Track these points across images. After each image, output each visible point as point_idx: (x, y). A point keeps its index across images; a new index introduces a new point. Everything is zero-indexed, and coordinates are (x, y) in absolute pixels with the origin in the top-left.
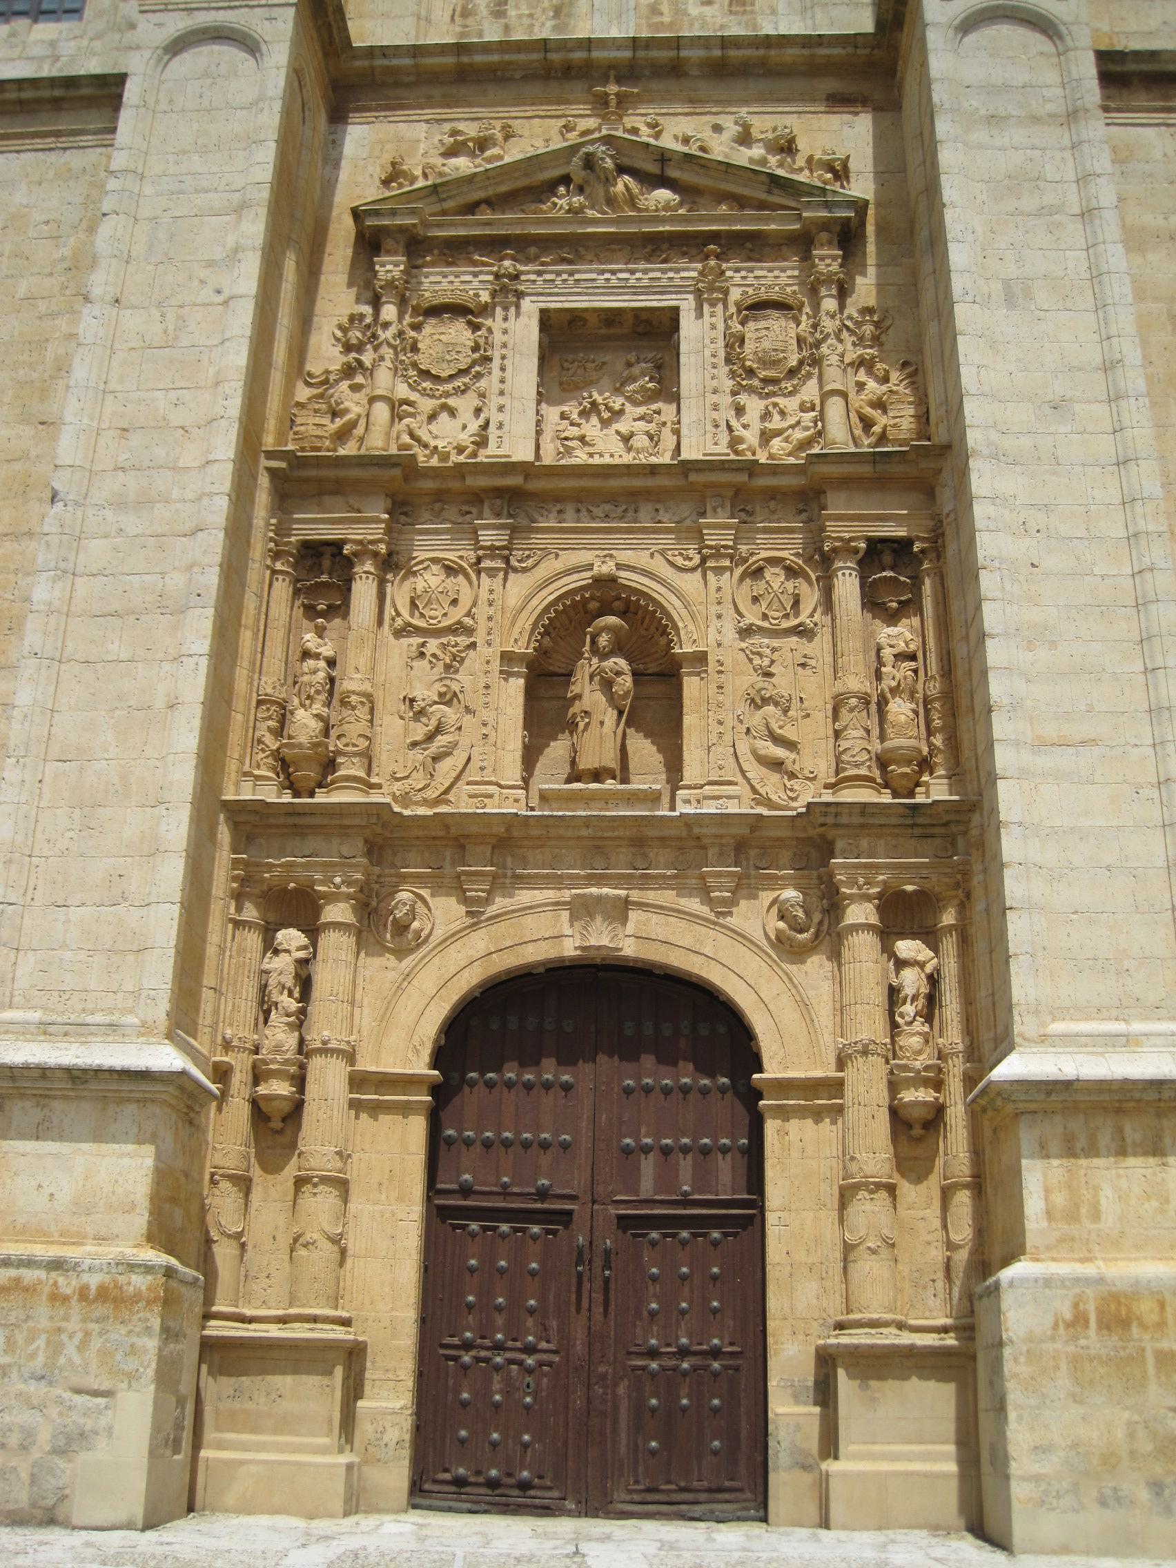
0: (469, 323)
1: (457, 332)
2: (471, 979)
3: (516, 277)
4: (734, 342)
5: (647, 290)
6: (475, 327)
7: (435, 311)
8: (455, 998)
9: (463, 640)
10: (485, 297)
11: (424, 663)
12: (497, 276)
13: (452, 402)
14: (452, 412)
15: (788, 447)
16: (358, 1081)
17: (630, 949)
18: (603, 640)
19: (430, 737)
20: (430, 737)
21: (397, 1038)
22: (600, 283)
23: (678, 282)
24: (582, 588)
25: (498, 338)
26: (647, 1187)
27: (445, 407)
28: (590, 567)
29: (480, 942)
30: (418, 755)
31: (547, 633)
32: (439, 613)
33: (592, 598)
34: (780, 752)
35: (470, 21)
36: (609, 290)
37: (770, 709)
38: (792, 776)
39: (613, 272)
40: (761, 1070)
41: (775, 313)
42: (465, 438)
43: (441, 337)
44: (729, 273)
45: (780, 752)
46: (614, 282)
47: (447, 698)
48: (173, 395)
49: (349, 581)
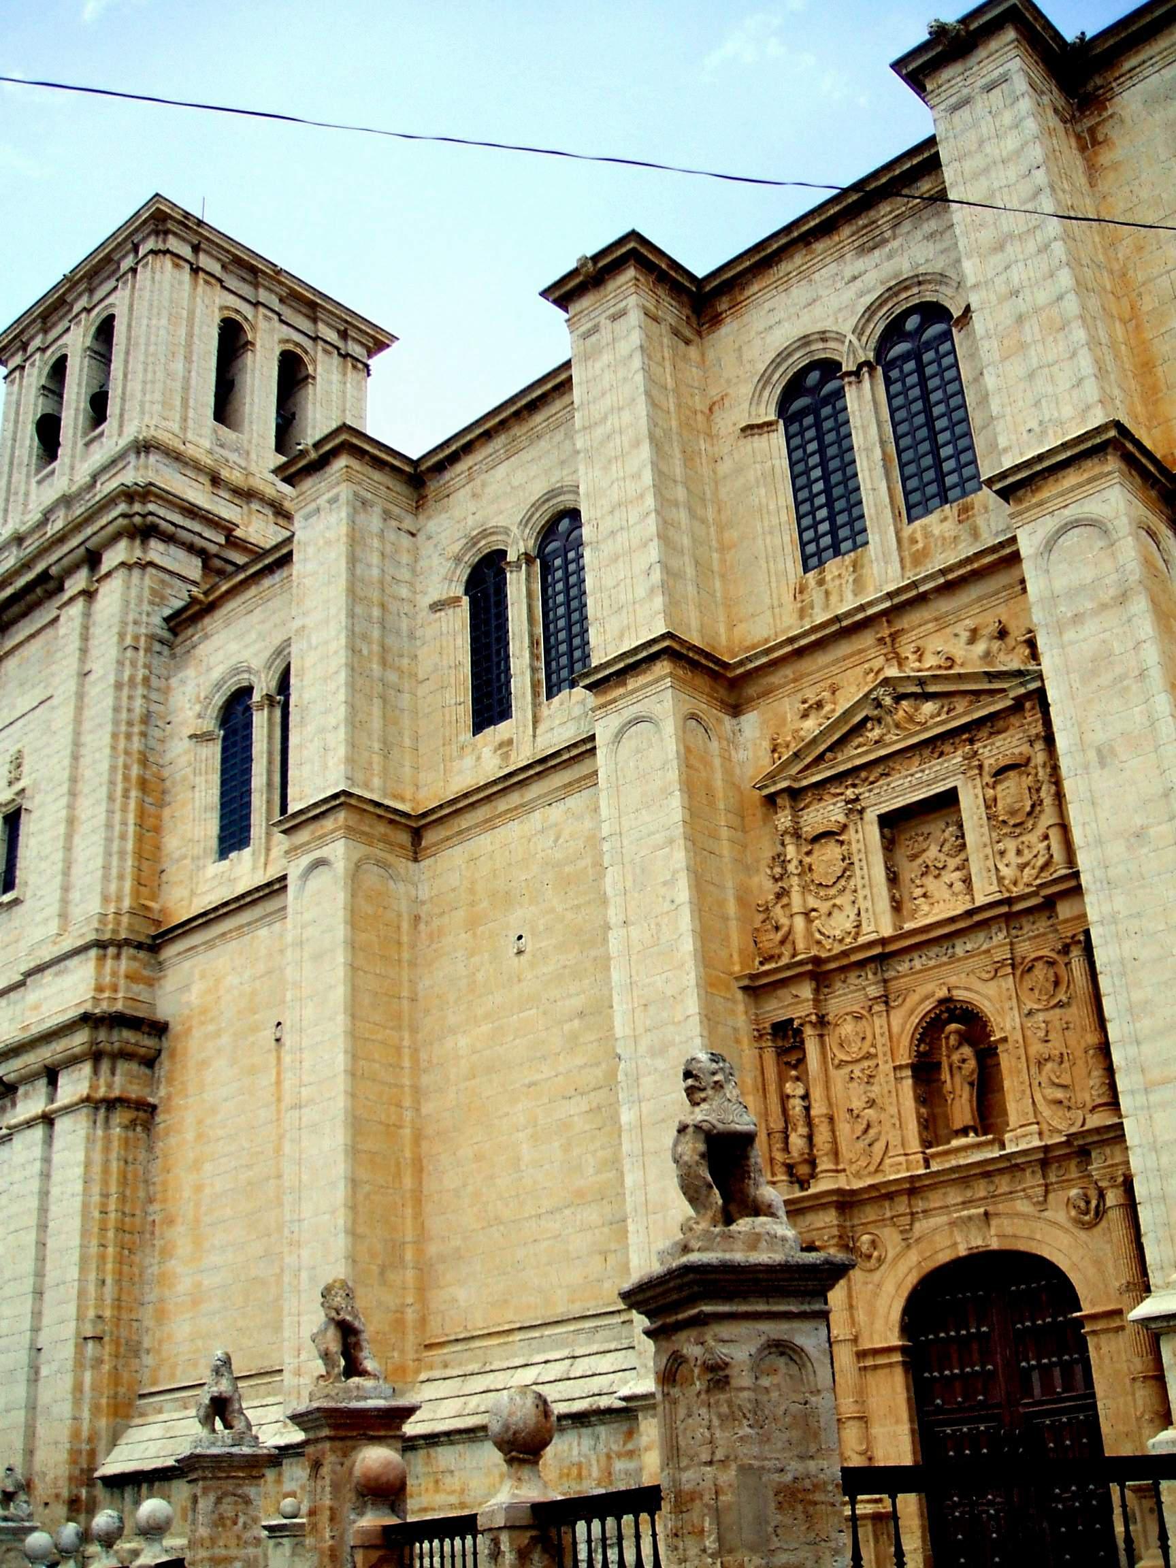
0: (837, 841)
1: (830, 852)
2: (912, 1280)
3: (857, 800)
4: (991, 803)
5: (935, 781)
6: (842, 843)
7: (816, 839)
8: (906, 1294)
9: (872, 1063)
10: (841, 818)
11: (854, 1084)
12: (847, 802)
13: (838, 901)
14: (840, 908)
15: (1035, 872)
16: (861, 1355)
17: (995, 1245)
18: (953, 1040)
19: (866, 1131)
20: (866, 1131)
21: (879, 1325)
22: (907, 785)
23: (951, 768)
24: (934, 1008)
25: (854, 847)
26: (1037, 1391)
27: (834, 905)
28: (933, 994)
29: (913, 1257)
30: (862, 1144)
31: (920, 1041)
32: (856, 1049)
33: (942, 1012)
34: (1059, 1094)
35: (805, 596)
36: (913, 788)
37: (1049, 1065)
38: (1069, 1108)
39: (912, 775)
40: (1080, 1310)
41: (1011, 774)
42: (849, 926)
43: (824, 858)
44: (981, 751)
45: (1059, 1094)
46: (914, 782)
47: (872, 1103)
48: (664, 976)
49: (802, 1042)
